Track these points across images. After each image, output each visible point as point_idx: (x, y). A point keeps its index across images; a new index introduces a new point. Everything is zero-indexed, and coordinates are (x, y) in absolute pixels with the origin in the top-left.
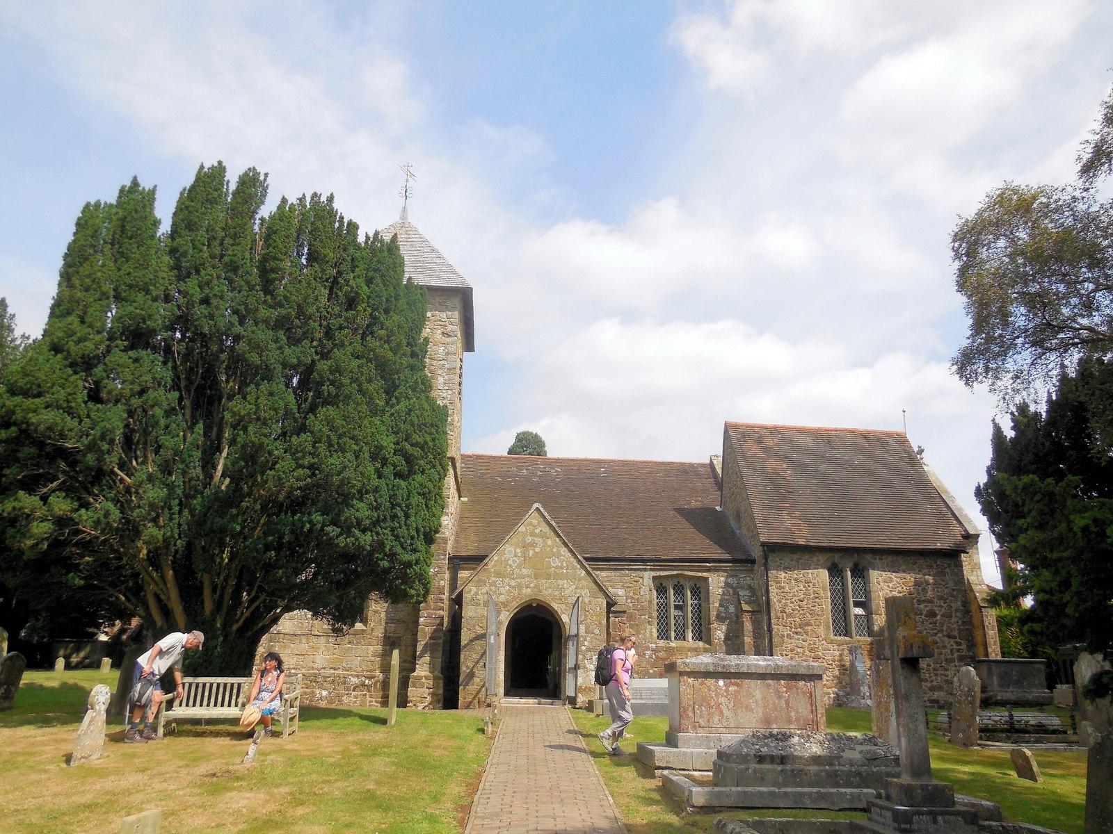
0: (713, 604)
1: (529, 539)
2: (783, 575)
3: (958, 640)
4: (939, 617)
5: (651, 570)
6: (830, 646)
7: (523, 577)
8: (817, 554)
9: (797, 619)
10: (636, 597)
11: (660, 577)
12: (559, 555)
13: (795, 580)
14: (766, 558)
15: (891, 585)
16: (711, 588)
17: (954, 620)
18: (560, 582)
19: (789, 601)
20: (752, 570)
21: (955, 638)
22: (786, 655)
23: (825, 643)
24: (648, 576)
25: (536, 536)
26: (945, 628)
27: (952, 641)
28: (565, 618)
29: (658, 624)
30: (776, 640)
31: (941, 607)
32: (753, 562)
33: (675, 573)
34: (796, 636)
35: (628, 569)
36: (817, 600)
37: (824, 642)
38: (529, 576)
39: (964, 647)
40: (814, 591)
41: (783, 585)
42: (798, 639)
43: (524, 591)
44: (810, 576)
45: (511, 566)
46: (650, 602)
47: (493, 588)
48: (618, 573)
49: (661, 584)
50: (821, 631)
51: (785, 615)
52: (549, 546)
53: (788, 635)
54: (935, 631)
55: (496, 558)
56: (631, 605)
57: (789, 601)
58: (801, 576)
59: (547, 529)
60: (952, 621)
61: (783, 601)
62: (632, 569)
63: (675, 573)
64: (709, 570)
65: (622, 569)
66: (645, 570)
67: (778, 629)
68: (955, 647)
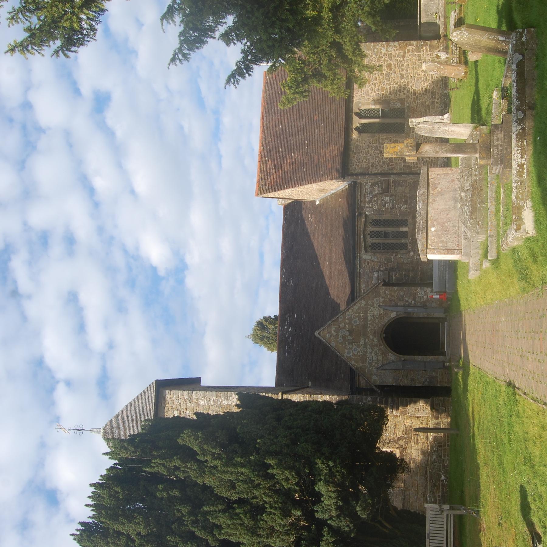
1: (340, 339)
4: (391, 62)
7: (365, 344)
8: (350, 140)
11: (365, 248)
14: (352, 175)
15: (370, 92)
17: (393, 52)
18: (369, 318)
20: (361, 183)
21: (404, 53)
25: (337, 335)
26: (399, 59)
27: (406, 55)
28: (393, 315)
32: (355, 183)
38: (365, 340)
39: (410, 48)
43: (375, 343)
47: (373, 364)
49: (370, 246)
52: (345, 325)
54: (401, 65)
55: (353, 362)
60: (394, 54)
68: (410, 53)
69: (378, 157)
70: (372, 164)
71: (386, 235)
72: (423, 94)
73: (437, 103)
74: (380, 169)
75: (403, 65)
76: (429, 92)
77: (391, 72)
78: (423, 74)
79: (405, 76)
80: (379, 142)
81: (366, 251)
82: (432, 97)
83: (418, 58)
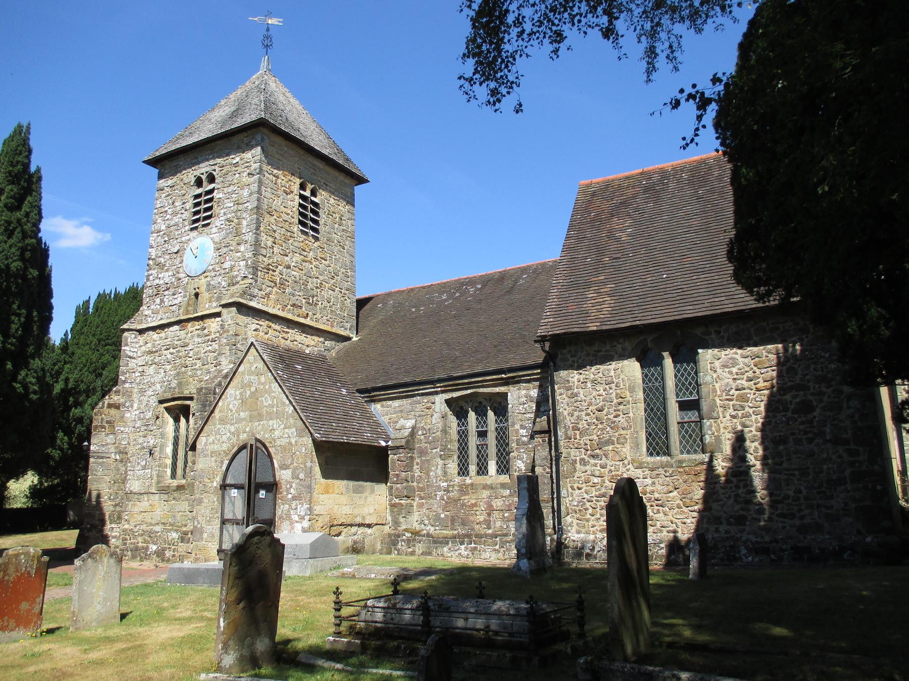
0: (513, 426)
2: (577, 376)
3: (852, 446)
5: (443, 392)
6: (640, 471)
8: (621, 340)
9: (596, 438)
10: (427, 427)
12: (269, 392)
13: (593, 381)
15: (734, 370)
16: (510, 406)
19: (583, 413)
22: (579, 489)
23: (632, 469)
24: (440, 400)
26: (828, 429)
29: (459, 457)
30: (564, 468)
31: (821, 393)
33: (469, 391)
34: (592, 461)
35: (418, 395)
36: (621, 407)
37: (630, 466)
40: (617, 394)
41: (576, 390)
42: (595, 465)
44: (612, 373)
45: (231, 411)
46: (445, 431)
48: (409, 400)
50: (626, 450)
51: (578, 432)
53: (582, 460)
54: (810, 435)
56: (422, 437)
57: (583, 413)
58: (600, 375)
59: (261, 365)
61: (576, 414)
62: (423, 394)
63: (469, 391)
64: (506, 382)
65: (413, 396)
66: (436, 393)
67: (569, 454)
69: (590, 404)
70: (576, 395)
71: (482, 434)
72: (737, 496)
73: (717, 530)
74: (566, 413)
75: (810, 441)
76: (742, 509)
77: (789, 414)
78: (791, 493)
79: (781, 447)
80: (620, 404)
81: (448, 402)
82: (731, 517)
83: (834, 477)
